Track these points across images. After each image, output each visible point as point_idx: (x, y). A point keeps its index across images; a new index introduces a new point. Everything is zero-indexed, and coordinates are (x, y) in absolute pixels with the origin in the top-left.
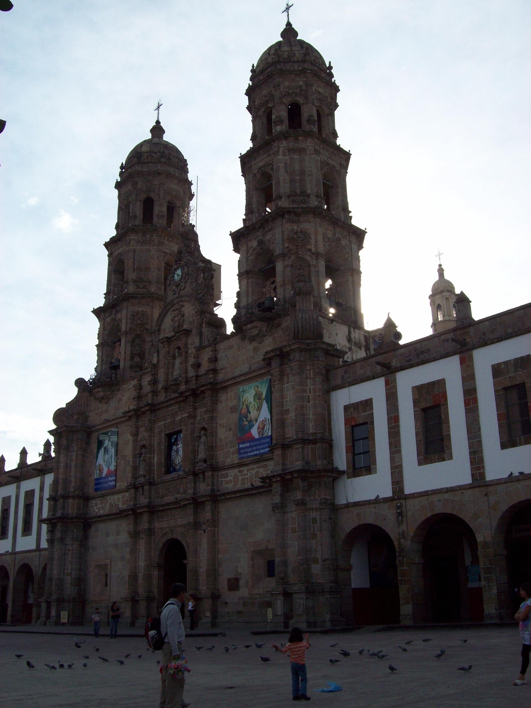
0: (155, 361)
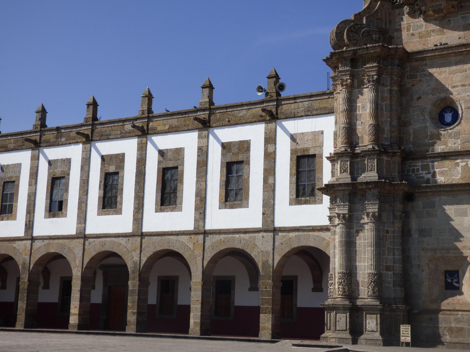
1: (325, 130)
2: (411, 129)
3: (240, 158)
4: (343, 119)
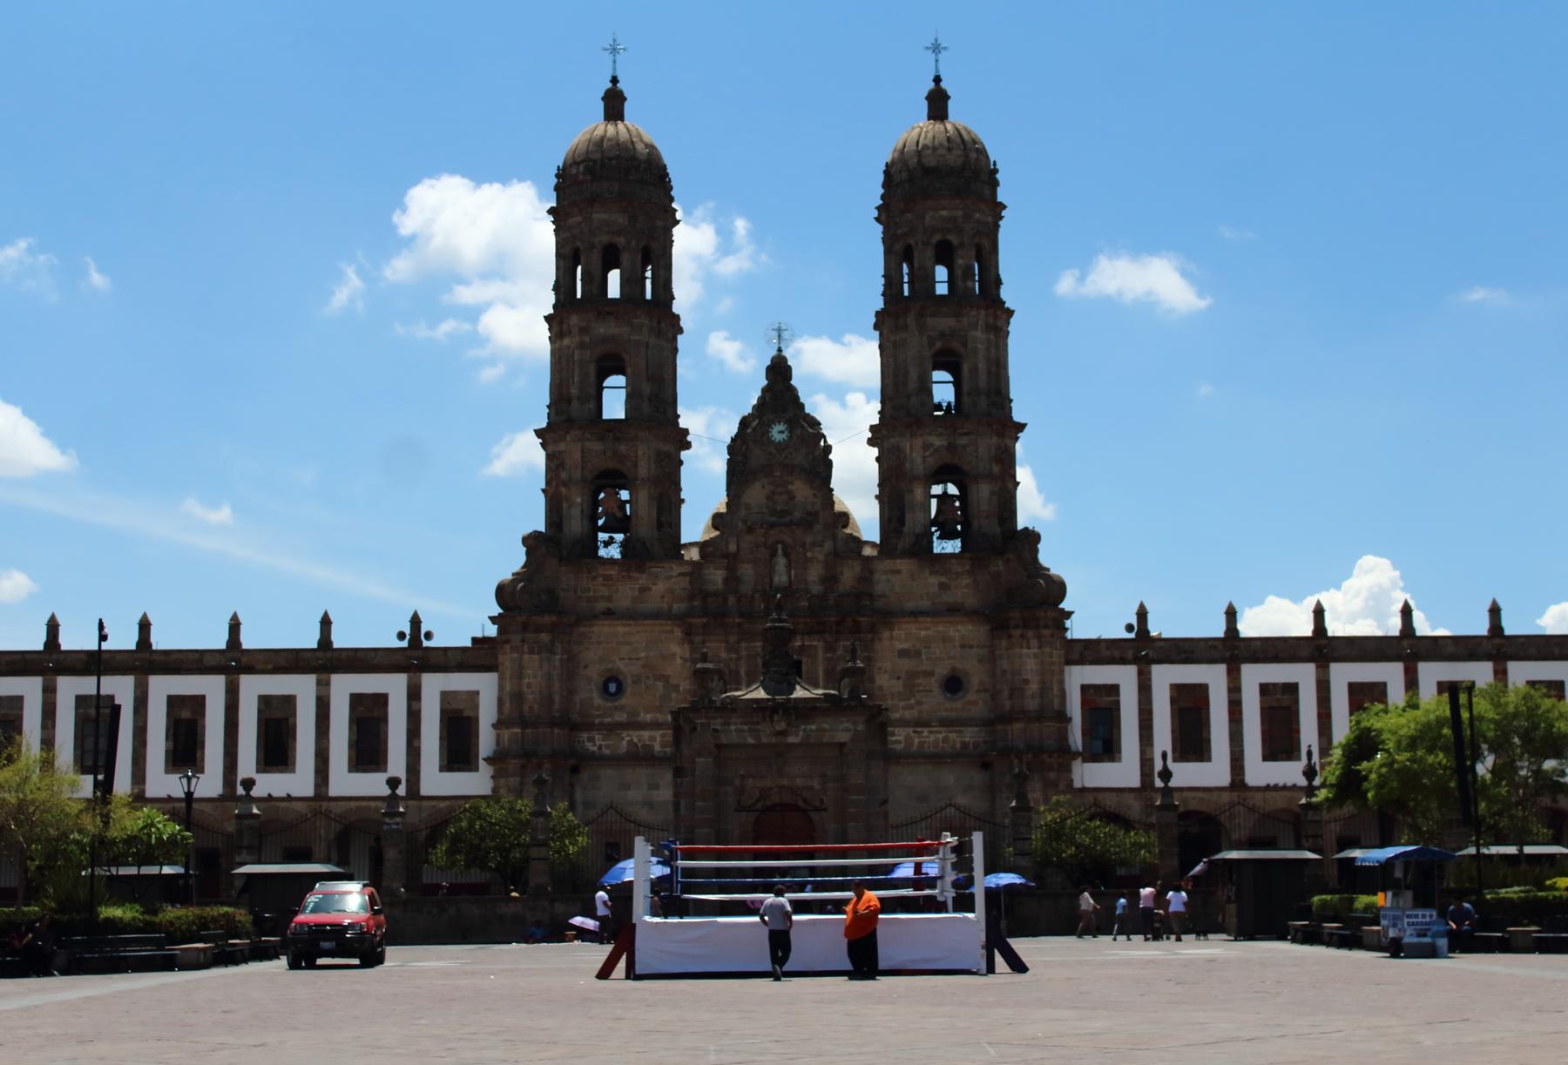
0: (733, 548)
2: (577, 699)
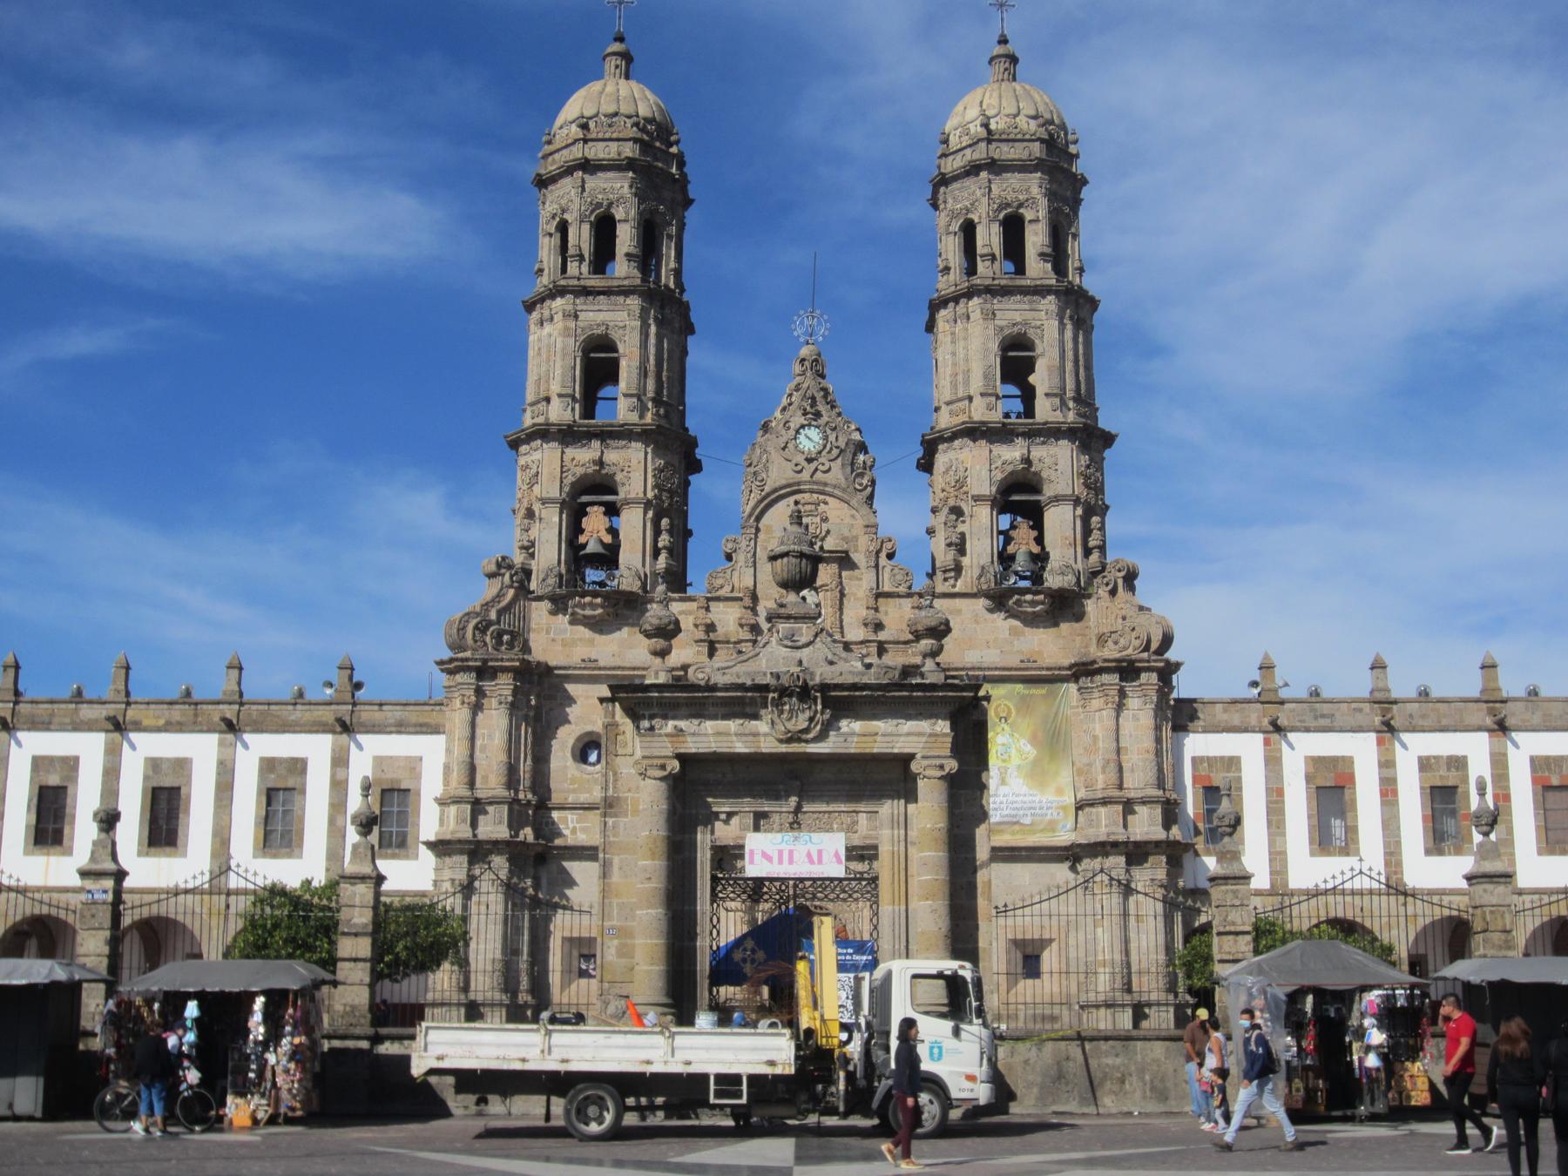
1: (431, 760)
3: (290, 784)
4: (460, 751)
